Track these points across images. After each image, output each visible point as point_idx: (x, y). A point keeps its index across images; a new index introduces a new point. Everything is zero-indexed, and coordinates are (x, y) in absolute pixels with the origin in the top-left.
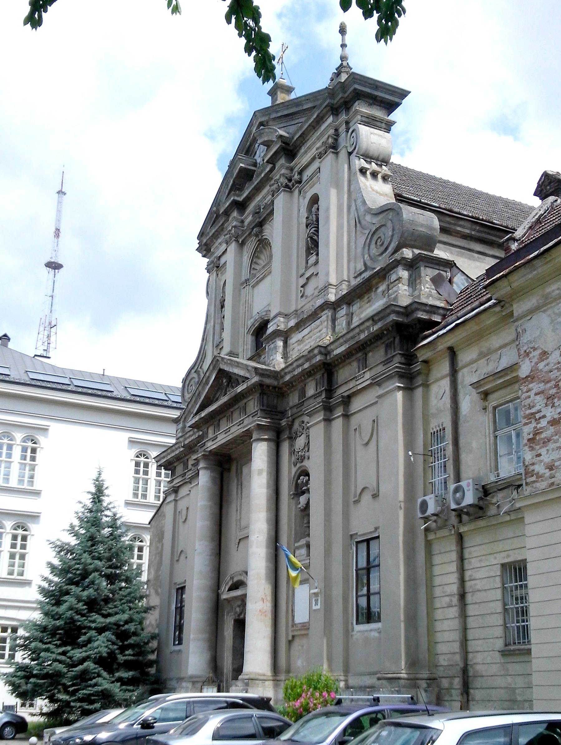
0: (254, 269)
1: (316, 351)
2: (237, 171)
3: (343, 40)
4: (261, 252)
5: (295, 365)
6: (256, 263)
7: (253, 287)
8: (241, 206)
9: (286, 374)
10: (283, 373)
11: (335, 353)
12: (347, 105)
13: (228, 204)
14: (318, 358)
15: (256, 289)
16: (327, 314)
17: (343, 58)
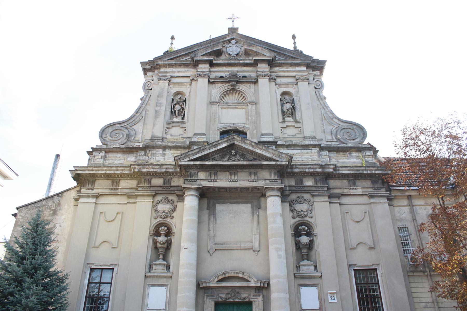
0: (221, 99)
1: (332, 167)
2: (217, 49)
3: (294, 41)
4: (228, 94)
5: (308, 167)
6: (223, 97)
7: (222, 108)
8: (212, 64)
9: (296, 168)
10: (294, 167)
11: (341, 172)
12: (314, 69)
13: (206, 59)
14: (331, 170)
15: (224, 111)
16: (315, 150)
17: (295, 47)
